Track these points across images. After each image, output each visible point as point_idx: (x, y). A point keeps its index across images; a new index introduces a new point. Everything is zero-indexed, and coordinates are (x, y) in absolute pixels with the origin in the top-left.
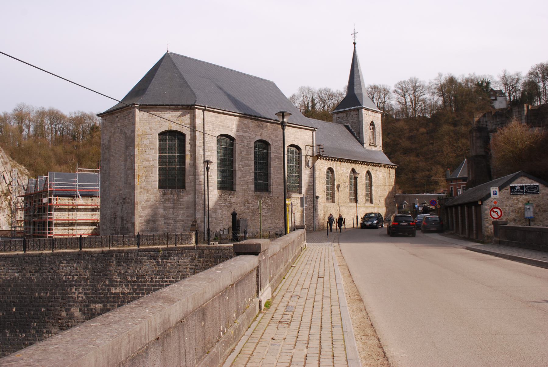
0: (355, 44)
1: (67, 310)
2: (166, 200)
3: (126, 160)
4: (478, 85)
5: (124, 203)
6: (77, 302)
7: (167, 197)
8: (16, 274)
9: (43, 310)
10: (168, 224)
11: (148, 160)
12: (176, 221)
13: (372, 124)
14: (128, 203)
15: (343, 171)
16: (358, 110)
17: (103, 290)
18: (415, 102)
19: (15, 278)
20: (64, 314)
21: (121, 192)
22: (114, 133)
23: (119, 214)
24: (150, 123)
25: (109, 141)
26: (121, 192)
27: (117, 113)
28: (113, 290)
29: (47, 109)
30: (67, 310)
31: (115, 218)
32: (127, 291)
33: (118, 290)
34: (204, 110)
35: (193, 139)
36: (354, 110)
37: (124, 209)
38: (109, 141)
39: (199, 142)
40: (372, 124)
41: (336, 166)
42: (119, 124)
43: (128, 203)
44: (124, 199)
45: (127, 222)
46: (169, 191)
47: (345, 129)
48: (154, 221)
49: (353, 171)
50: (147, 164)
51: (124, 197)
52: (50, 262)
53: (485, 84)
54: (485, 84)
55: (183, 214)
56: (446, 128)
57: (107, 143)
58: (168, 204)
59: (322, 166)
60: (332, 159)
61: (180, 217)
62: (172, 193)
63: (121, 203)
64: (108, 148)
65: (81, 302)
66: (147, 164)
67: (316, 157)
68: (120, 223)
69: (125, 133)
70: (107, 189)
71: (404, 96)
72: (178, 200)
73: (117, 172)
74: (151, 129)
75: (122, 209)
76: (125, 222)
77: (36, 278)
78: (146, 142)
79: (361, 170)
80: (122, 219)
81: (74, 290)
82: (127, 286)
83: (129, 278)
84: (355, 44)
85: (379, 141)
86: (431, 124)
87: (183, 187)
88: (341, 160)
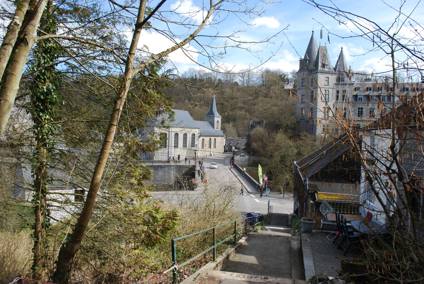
4: (281, 76)
13: (218, 121)
15: (207, 139)
18: (248, 82)
35: (169, 135)
39: (170, 136)
40: (218, 121)
41: (204, 138)
47: (209, 123)
49: (210, 139)
53: (283, 76)
54: (283, 76)
56: (260, 98)
59: (201, 138)
60: (204, 136)
67: (199, 137)
71: (243, 78)
79: (213, 139)
85: (220, 127)
86: (254, 95)
88: (206, 136)
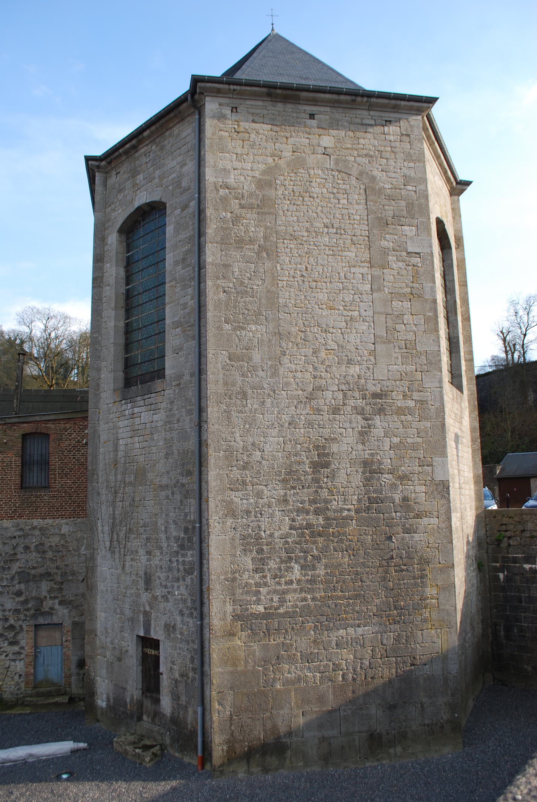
3: (378, 262)
5: (381, 411)
21: (355, 370)
23: (346, 446)
26: (355, 370)
27: (315, 102)
31: (322, 462)
37: (378, 432)
43: (401, 411)
44: (375, 396)
45: (403, 478)
51: (372, 388)
57: (249, 187)
63: (360, 412)
64: (264, 207)
68: (357, 480)
70: (257, 356)
73: (322, 296)
75: (361, 433)
76: (387, 478)
80: (370, 469)
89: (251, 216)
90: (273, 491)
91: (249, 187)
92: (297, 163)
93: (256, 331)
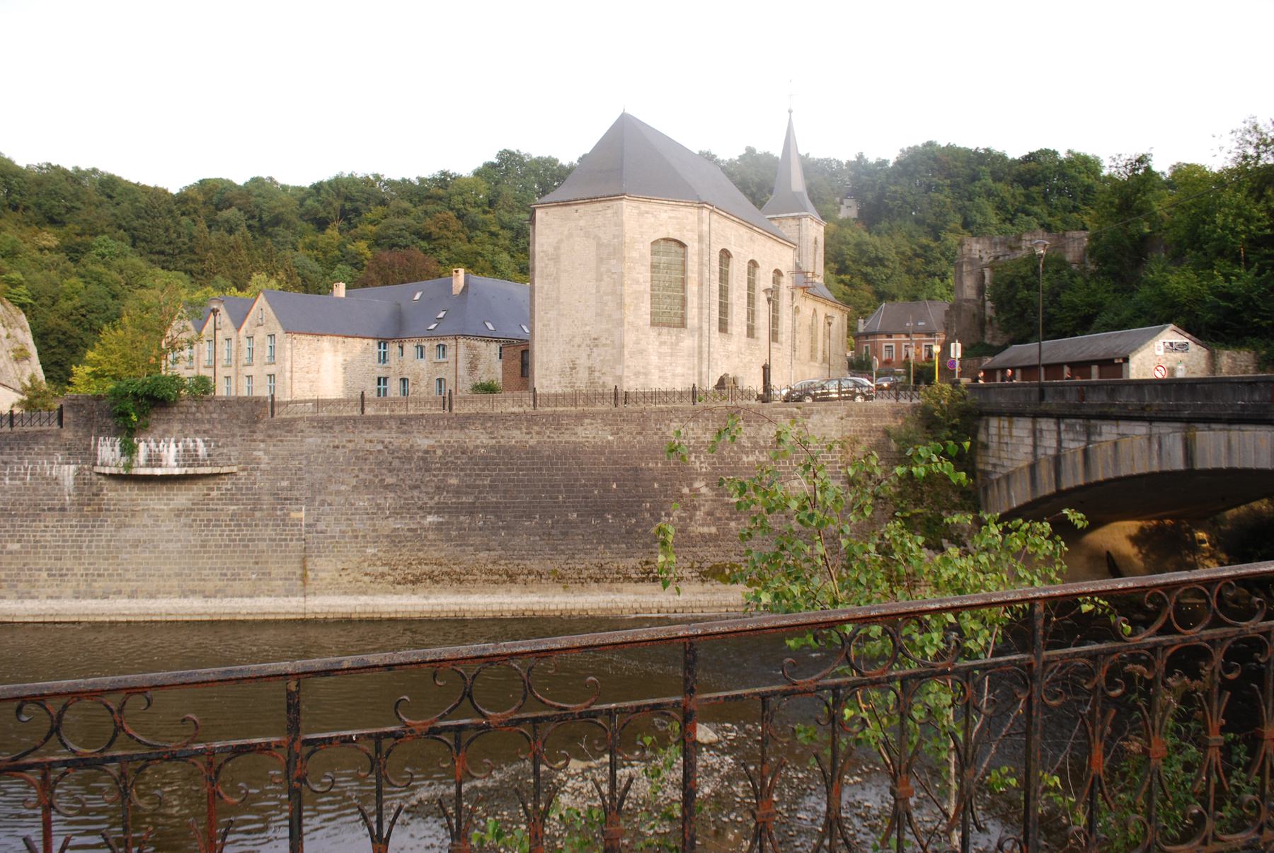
0: (790, 112)
1: (690, 486)
2: (662, 344)
3: (599, 279)
5: (597, 346)
6: (700, 474)
7: (664, 338)
8: (610, 438)
9: (656, 485)
10: (664, 379)
11: (638, 282)
12: (674, 375)
14: (604, 345)
16: (799, 218)
17: (732, 458)
19: (608, 442)
20: (686, 490)
21: (588, 328)
22: (570, 236)
23: (583, 361)
24: (641, 226)
25: (557, 248)
26: (588, 328)
28: (745, 459)
29: (54, 164)
30: (690, 486)
32: (762, 459)
33: (751, 458)
34: (711, 211)
36: (794, 218)
37: (594, 355)
38: (557, 248)
42: (582, 223)
43: (604, 345)
46: (665, 330)
48: (646, 374)
50: (635, 287)
51: (594, 336)
52: (657, 421)
55: (684, 365)
57: (551, 250)
58: (665, 349)
61: (679, 370)
62: (669, 333)
64: (556, 259)
65: (706, 474)
66: (635, 287)
68: (586, 375)
69: (597, 238)
72: (677, 344)
74: (642, 233)
76: (597, 374)
77: (639, 442)
78: (635, 254)
80: (591, 370)
81: (693, 459)
82: (761, 452)
83: (762, 444)
84: (790, 112)
87: (683, 324)
89: (551, 263)
90: (556, 379)
91: (551, 250)
92: (570, 236)
93: (552, 314)
